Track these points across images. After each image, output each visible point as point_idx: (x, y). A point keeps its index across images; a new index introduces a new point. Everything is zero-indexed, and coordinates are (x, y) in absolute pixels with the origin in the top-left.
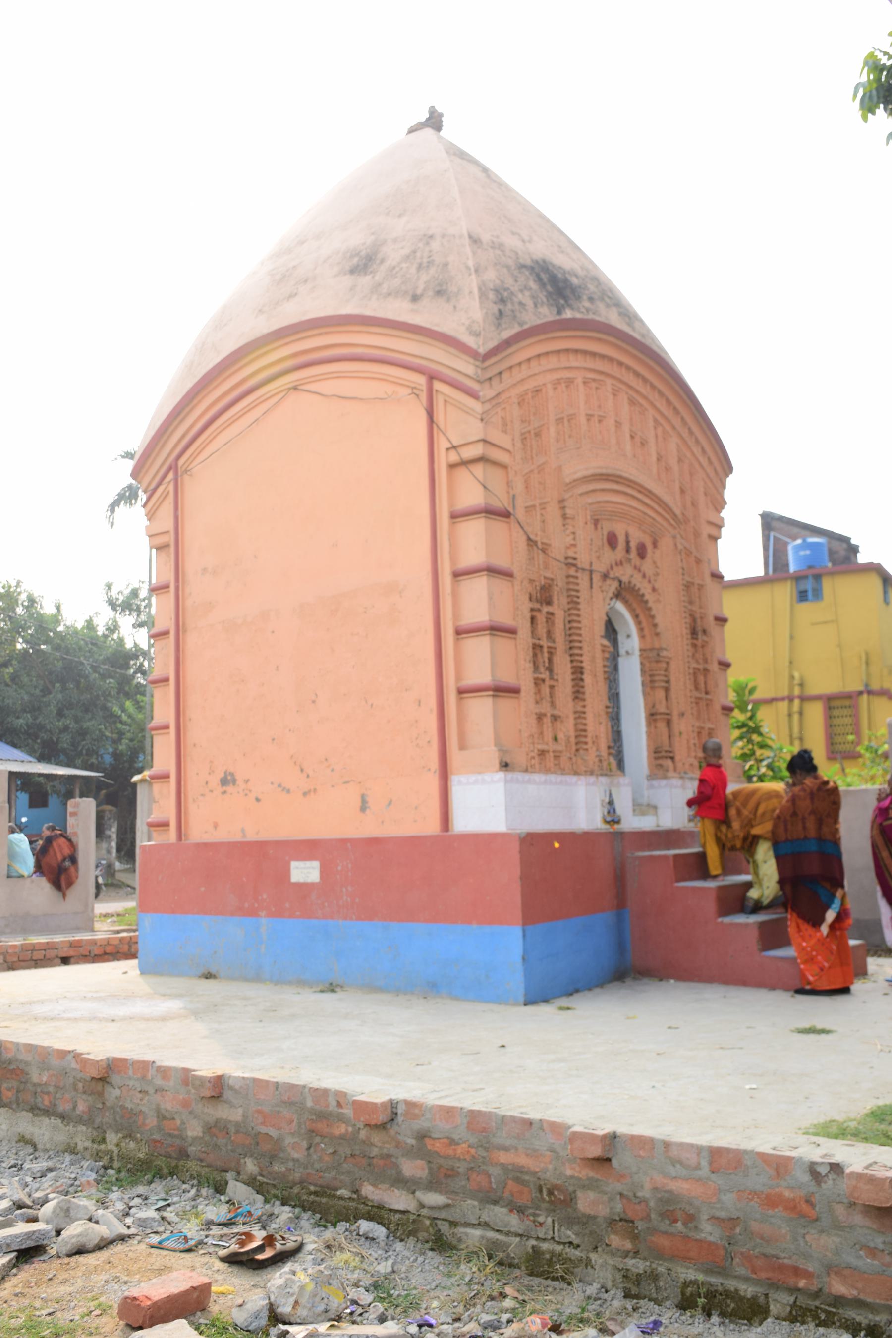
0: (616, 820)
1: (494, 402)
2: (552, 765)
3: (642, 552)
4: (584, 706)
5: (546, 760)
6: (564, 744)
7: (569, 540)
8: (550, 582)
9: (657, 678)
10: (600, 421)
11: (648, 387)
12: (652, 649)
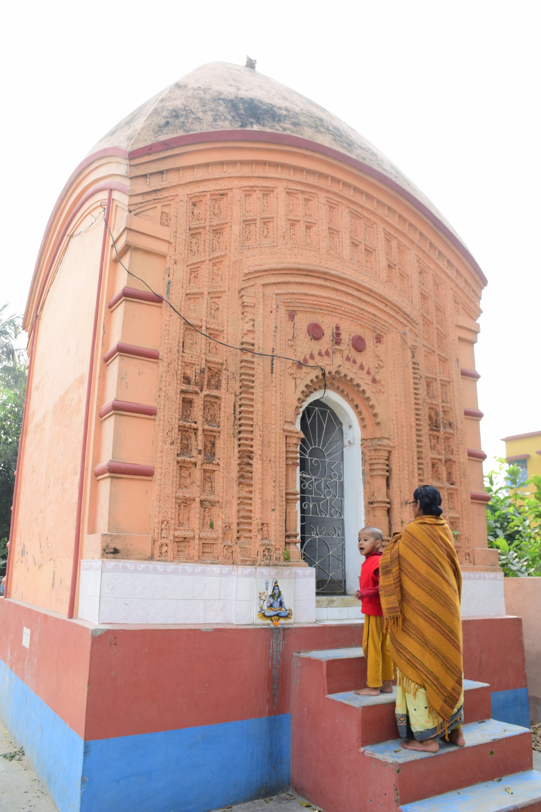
0: (283, 614)
1: (149, 198)
2: (196, 553)
3: (359, 344)
4: (251, 492)
5: (178, 547)
6: (220, 531)
7: (248, 327)
8: (219, 366)
9: (375, 467)
10: (308, 227)
11: (375, 204)
12: (372, 439)
